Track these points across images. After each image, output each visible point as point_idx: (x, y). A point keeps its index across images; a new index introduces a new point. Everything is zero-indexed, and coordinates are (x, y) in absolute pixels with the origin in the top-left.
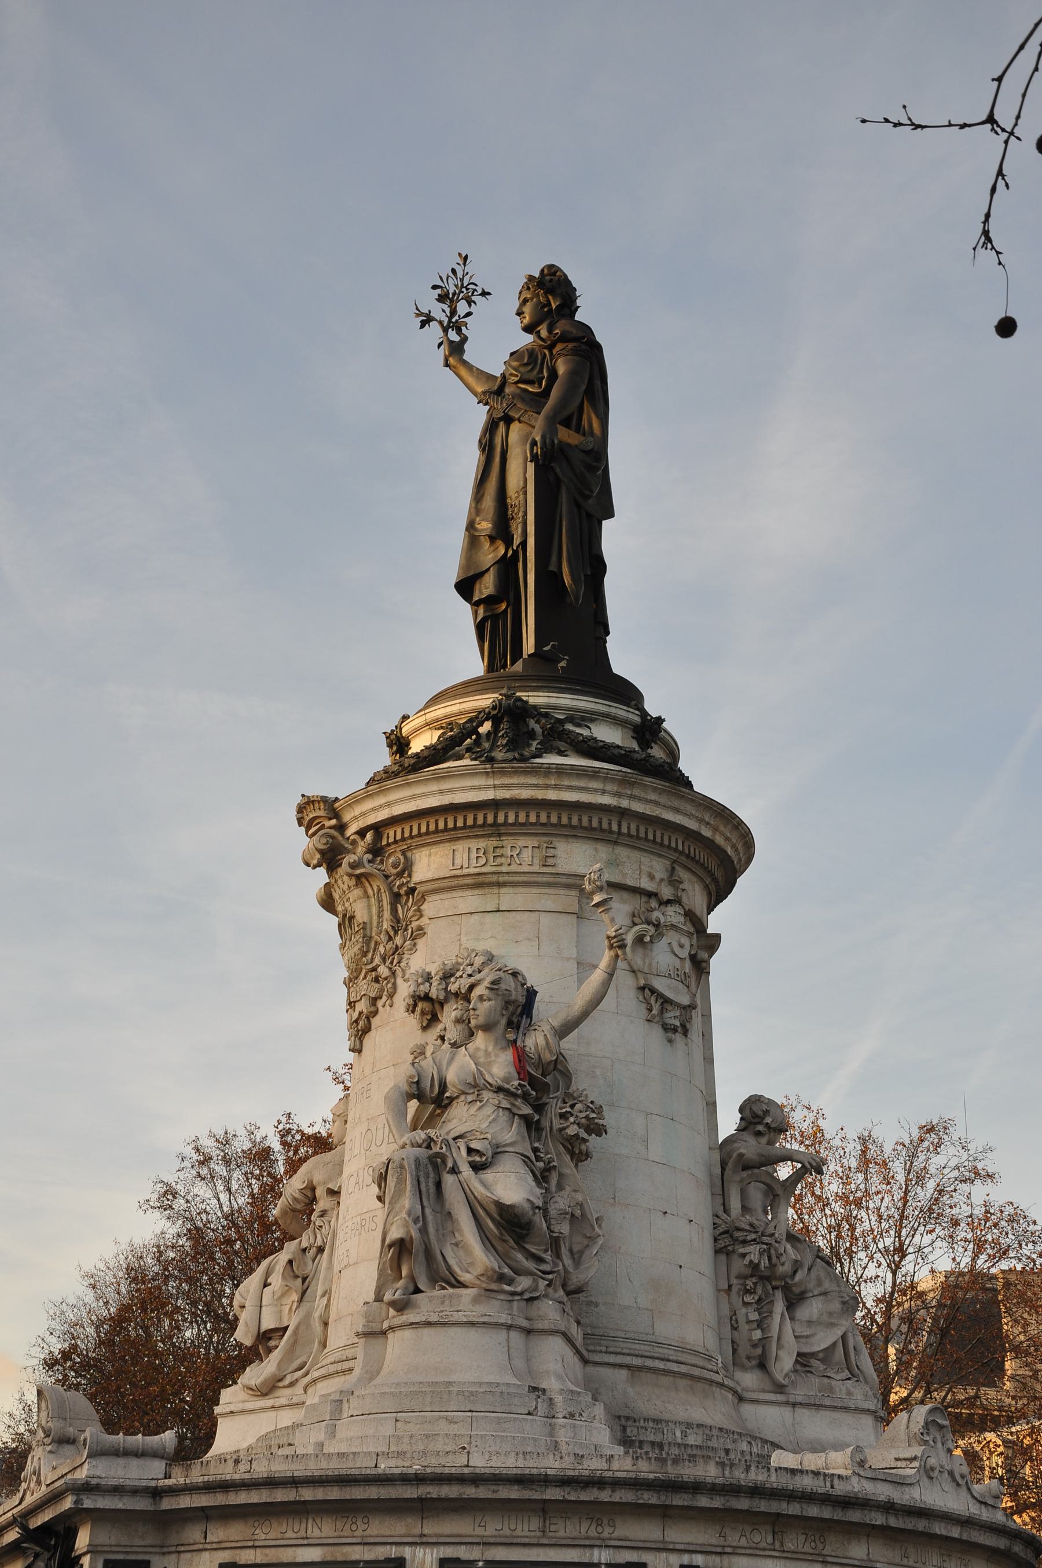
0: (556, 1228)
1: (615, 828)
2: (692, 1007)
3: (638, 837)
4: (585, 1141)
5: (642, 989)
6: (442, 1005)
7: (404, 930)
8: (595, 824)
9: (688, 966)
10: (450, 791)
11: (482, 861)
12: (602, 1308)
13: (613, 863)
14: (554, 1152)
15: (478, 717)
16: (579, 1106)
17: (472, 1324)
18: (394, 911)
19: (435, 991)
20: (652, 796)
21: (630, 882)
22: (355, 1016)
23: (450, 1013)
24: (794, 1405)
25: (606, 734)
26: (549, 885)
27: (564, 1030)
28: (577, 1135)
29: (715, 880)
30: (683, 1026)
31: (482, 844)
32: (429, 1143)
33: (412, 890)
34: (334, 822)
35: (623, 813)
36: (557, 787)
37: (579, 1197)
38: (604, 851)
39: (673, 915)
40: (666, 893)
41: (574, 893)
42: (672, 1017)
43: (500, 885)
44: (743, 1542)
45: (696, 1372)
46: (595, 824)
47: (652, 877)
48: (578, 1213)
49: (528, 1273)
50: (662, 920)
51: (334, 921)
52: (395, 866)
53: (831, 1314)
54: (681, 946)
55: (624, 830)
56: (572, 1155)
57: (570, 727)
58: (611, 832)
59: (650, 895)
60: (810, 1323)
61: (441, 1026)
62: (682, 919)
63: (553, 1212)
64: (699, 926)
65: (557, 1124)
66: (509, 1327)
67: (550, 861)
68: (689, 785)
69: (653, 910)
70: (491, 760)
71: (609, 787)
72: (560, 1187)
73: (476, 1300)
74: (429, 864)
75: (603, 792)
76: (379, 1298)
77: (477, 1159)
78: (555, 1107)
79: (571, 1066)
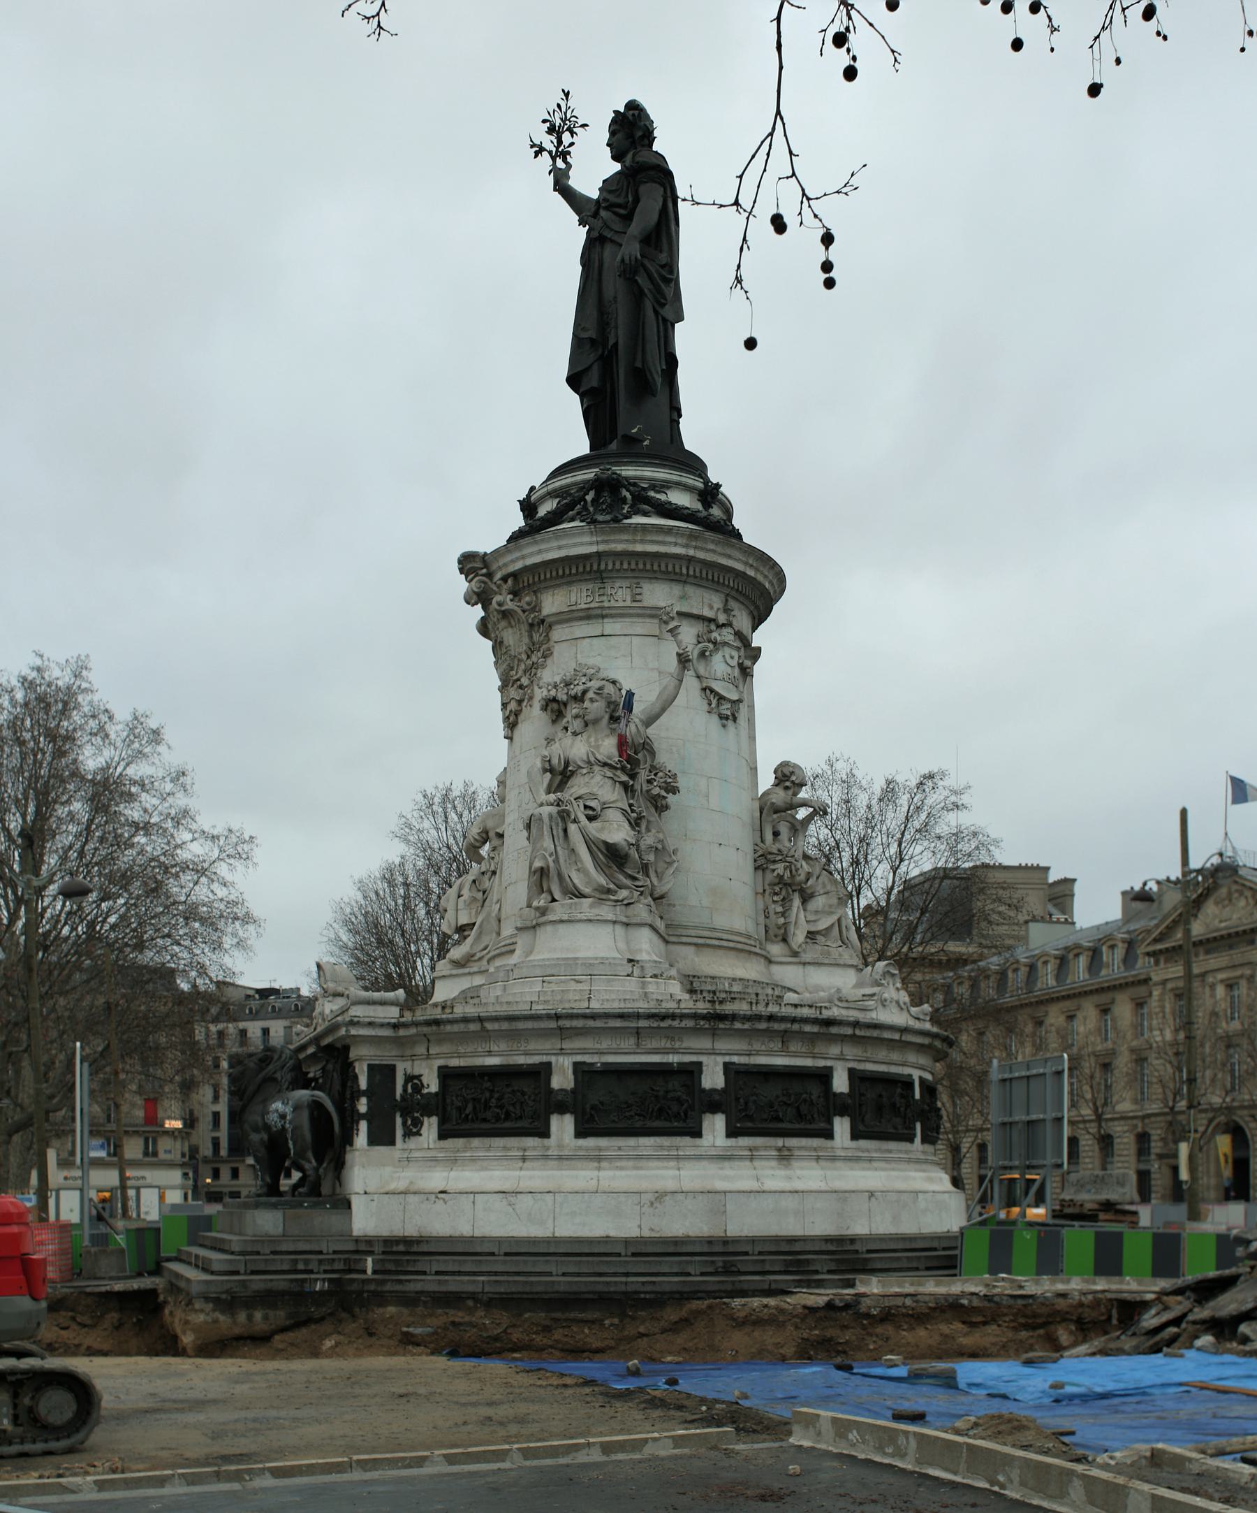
0: (646, 857)
1: (684, 571)
2: (740, 701)
3: (701, 578)
4: (665, 798)
5: (704, 689)
6: (565, 704)
7: (539, 650)
8: (670, 569)
9: (737, 672)
10: (567, 546)
11: (589, 599)
12: (678, 907)
13: (683, 597)
14: (643, 807)
15: (585, 487)
16: (660, 774)
17: (590, 921)
18: (531, 637)
19: (562, 696)
20: (711, 546)
21: (695, 612)
22: (507, 713)
23: (573, 710)
24: (804, 964)
25: (680, 499)
26: (639, 616)
27: (649, 722)
28: (659, 795)
29: (757, 607)
30: (733, 715)
31: (590, 586)
32: (559, 803)
33: (543, 621)
34: (484, 571)
35: (690, 559)
36: (642, 542)
37: (661, 836)
38: (677, 589)
39: (727, 635)
40: (722, 618)
41: (656, 621)
42: (726, 709)
43: (603, 617)
44: (763, 1048)
45: (740, 946)
46: (670, 569)
47: (711, 607)
48: (660, 847)
49: (627, 887)
50: (719, 639)
51: (490, 643)
52: (529, 604)
53: (830, 906)
54: (732, 658)
55: (691, 573)
56: (656, 808)
57: (652, 494)
58: (681, 574)
59: (710, 620)
60: (816, 912)
61: (565, 720)
62: (732, 637)
63: (643, 847)
64: (745, 642)
65: (645, 787)
66: (615, 922)
67: (638, 598)
68: (739, 536)
69: (711, 632)
70: (594, 522)
71: (679, 541)
72: (648, 830)
73: (591, 906)
74: (552, 603)
75: (676, 544)
76: (529, 906)
77: (591, 813)
78: (643, 775)
79: (656, 746)
